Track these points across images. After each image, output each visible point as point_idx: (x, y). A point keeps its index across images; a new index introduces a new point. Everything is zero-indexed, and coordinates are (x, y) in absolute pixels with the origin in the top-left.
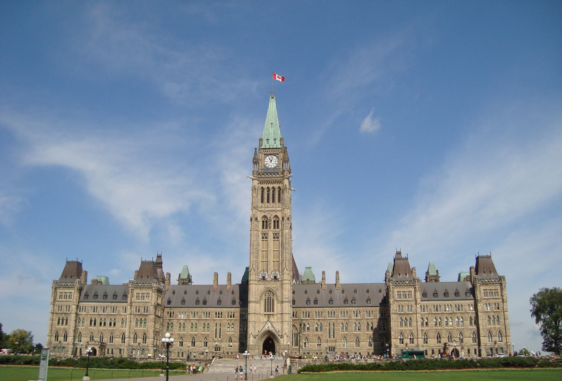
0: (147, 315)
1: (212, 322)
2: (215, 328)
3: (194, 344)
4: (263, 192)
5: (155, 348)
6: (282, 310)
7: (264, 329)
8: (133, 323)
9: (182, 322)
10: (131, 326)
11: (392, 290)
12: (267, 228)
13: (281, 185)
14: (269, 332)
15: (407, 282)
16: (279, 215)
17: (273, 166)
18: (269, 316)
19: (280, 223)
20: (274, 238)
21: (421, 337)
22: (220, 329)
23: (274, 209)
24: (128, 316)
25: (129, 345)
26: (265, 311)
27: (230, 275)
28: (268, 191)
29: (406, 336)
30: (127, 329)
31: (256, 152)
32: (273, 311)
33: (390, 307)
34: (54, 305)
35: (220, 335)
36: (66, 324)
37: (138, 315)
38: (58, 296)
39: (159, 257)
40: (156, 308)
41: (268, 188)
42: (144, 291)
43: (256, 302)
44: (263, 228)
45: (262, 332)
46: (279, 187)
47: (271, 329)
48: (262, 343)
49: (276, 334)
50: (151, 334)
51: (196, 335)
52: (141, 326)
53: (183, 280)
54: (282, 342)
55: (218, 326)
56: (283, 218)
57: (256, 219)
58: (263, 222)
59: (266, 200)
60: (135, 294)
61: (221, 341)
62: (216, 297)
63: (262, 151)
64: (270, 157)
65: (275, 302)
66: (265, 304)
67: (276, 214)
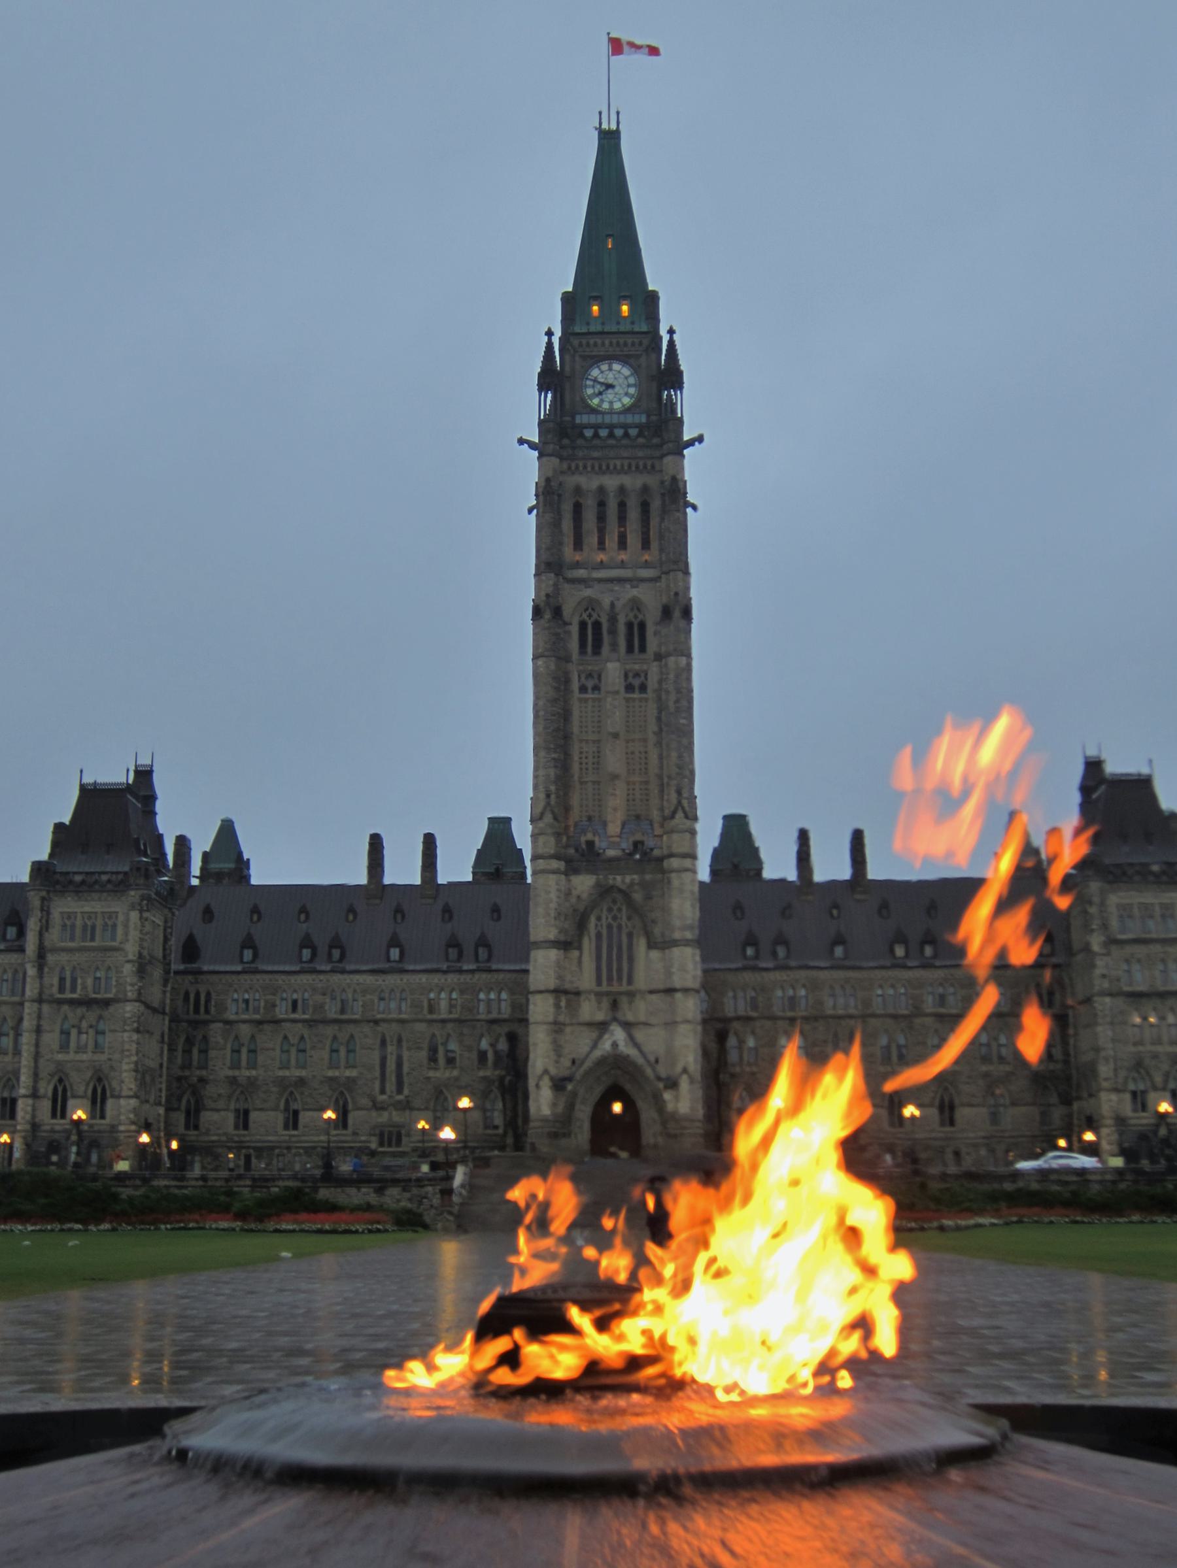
0: (107, 1003)
1: (367, 1029)
2: (376, 1056)
3: (293, 1120)
6: (669, 974)
7: (597, 1053)
8: (51, 1039)
9: (245, 1030)
11: (1096, 899)
13: (651, 480)
14: (616, 1062)
15: (1155, 868)
16: (651, 599)
17: (617, 406)
18: (615, 1005)
19: (650, 630)
20: (629, 688)
24: (29, 1009)
25: (35, 1126)
26: (599, 983)
27: (429, 842)
28: (602, 504)
29: (1158, 1079)
30: (26, 1060)
31: (550, 345)
32: (630, 982)
33: (1093, 966)
37: (71, 1002)
39: (144, 775)
40: (142, 970)
41: (601, 490)
42: (94, 905)
43: (564, 945)
45: (588, 1064)
46: (645, 489)
47: (625, 1049)
49: (649, 1072)
50: (127, 1082)
51: (301, 1082)
52: (80, 1049)
53: (219, 876)
54: (670, 1107)
55: (390, 1048)
56: (667, 613)
57: (557, 612)
58: (583, 625)
60: (56, 915)
61: (406, 1106)
63: (576, 342)
64: (605, 367)
65: (641, 944)
67: (635, 592)
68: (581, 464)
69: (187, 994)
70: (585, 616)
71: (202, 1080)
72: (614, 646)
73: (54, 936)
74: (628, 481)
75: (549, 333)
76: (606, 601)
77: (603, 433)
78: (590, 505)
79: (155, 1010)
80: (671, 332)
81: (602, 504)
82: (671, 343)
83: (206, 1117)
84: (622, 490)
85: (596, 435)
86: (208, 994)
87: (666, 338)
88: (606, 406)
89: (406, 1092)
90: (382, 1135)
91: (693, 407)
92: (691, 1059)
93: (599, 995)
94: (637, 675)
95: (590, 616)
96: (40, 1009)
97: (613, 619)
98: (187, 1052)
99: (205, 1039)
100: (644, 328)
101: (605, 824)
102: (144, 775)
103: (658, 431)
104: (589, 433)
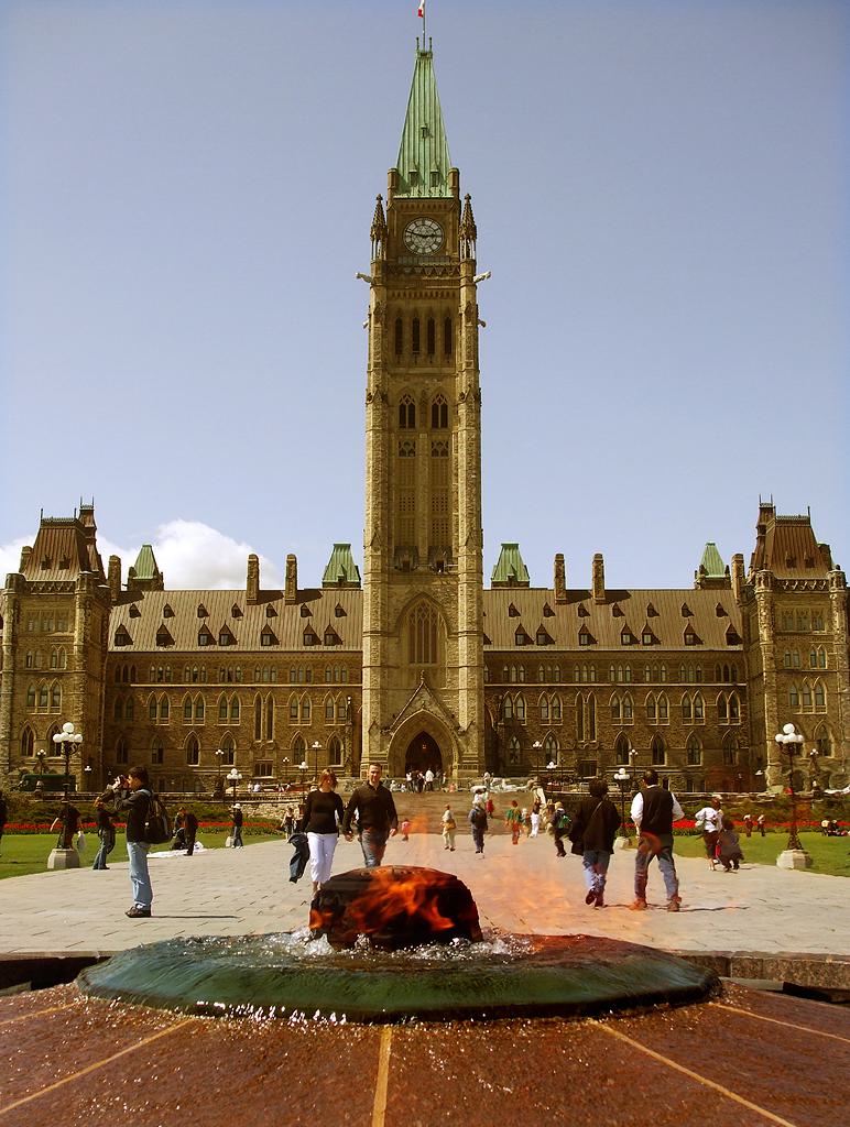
4: (399, 323)
5: (88, 769)
10: (16, 707)
12: (412, 425)
20: (435, 453)
22: (270, 713)
23: (436, 370)
27: (292, 563)
28: (416, 323)
31: (380, 206)
32: (434, 661)
35: (270, 730)
41: (416, 310)
47: (434, 709)
48: (404, 749)
52: (42, 705)
58: (402, 407)
59: (407, 347)
66: (412, 644)
68: (402, 292)
69: (119, 667)
70: (404, 401)
71: (128, 728)
72: (424, 423)
73: (23, 623)
74: (435, 304)
75: (380, 199)
76: (419, 391)
77: (418, 270)
78: (407, 320)
79: (95, 678)
81: (416, 323)
83: (131, 753)
84: (431, 309)
85: (413, 272)
86: (134, 668)
87: (464, 202)
88: (420, 251)
89: (274, 737)
90: (257, 766)
91: (482, 251)
92: (476, 716)
93: (411, 672)
95: (407, 401)
96: (13, 678)
97: (424, 403)
98: (119, 707)
99: (131, 698)
100: (449, 194)
101: (417, 549)
102: (87, 512)
103: (453, 269)
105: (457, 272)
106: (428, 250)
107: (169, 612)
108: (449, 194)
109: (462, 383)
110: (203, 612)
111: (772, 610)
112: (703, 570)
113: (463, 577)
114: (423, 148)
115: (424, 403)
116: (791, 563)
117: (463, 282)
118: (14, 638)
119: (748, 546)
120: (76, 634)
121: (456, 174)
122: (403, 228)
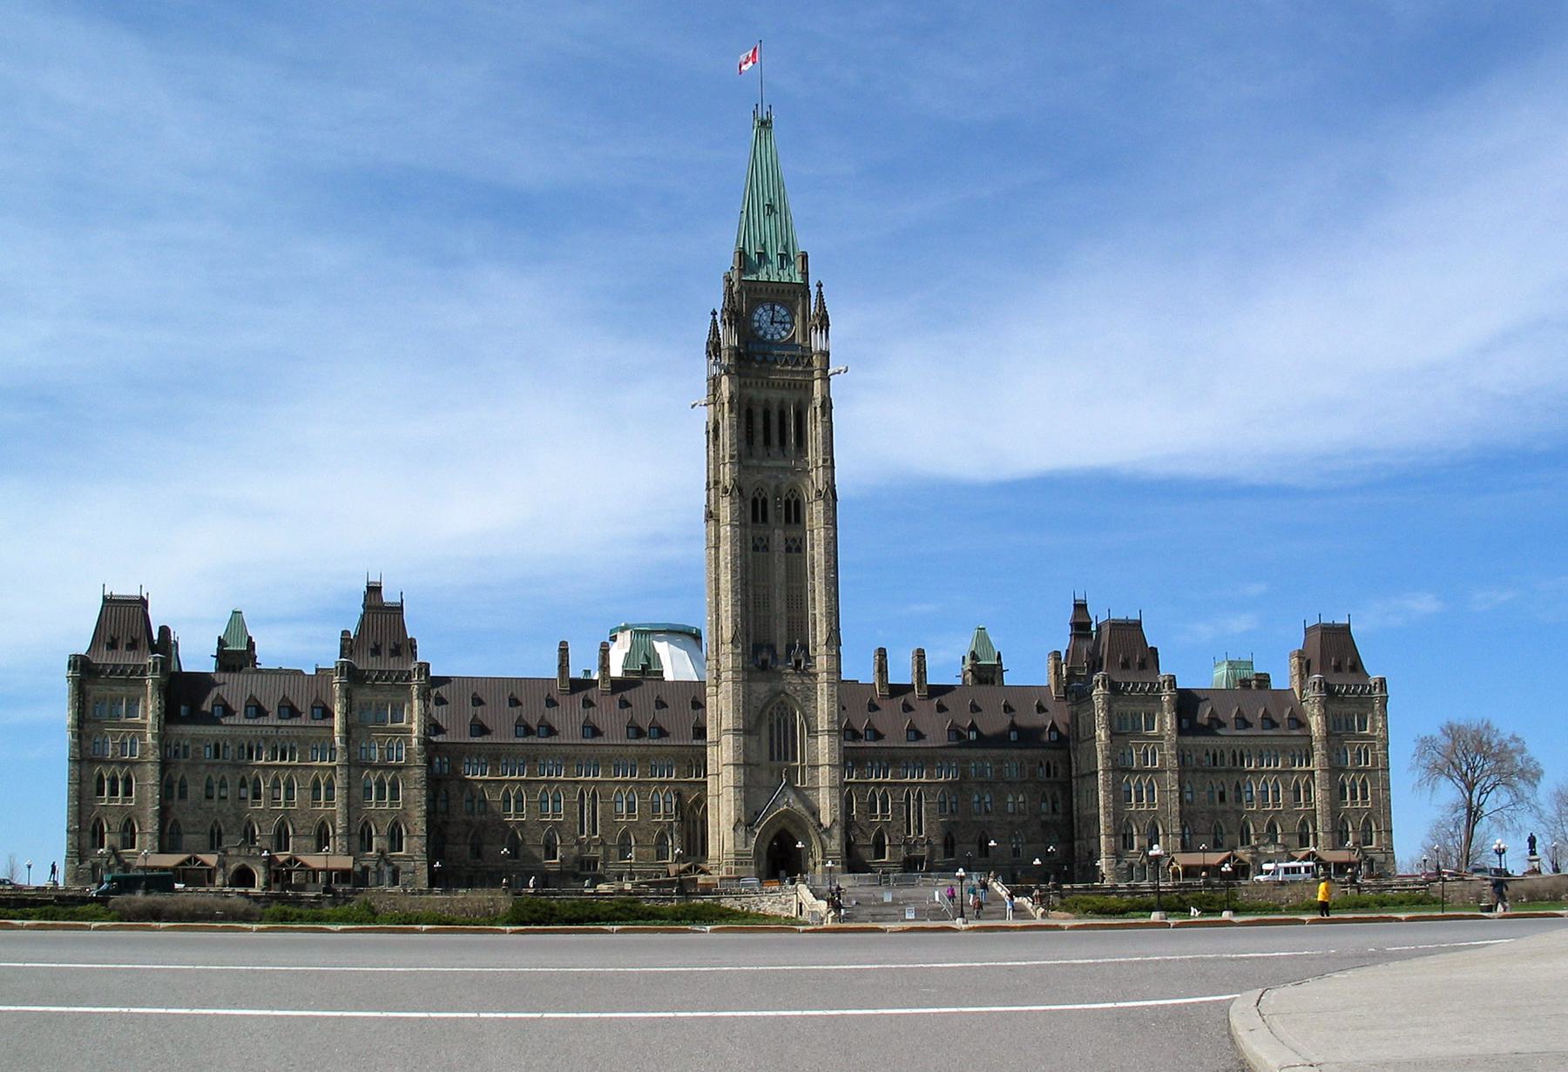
0: (400, 768)
12: (765, 519)
20: (789, 550)
21: (1177, 830)
26: (772, 759)
34: (79, 737)
36: (128, 792)
38: (90, 705)
41: (767, 401)
44: (755, 519)
48: (766, 846)
58: (755, 501)
62: (580, 714)
72: (778, 517)
73: (356, 713)
76: (773, 484)
78: (759, 411)
80: (820, 286)
82: (820, 294)
85: (765, 360)
94: (794, 540)
97: (778, 493)
100: (798, 279)
101: (772, 648)
104: (759, 358)
105: (810, 363)
106: (777, 337)
107: (478, 701)
108: (798, 279)
109: (818, 477)
110: (514, 702)
111: (1109, 711)
112: (974, 656)
113: (823, 677)
114: (768, 226)
115: (778, 493)
116: (1125, 665)
117: (817, 374)
118: (347, 729)
119: (1063, 643)
120: (415, 726)
121: (805, 257)
122: (751, 310)
